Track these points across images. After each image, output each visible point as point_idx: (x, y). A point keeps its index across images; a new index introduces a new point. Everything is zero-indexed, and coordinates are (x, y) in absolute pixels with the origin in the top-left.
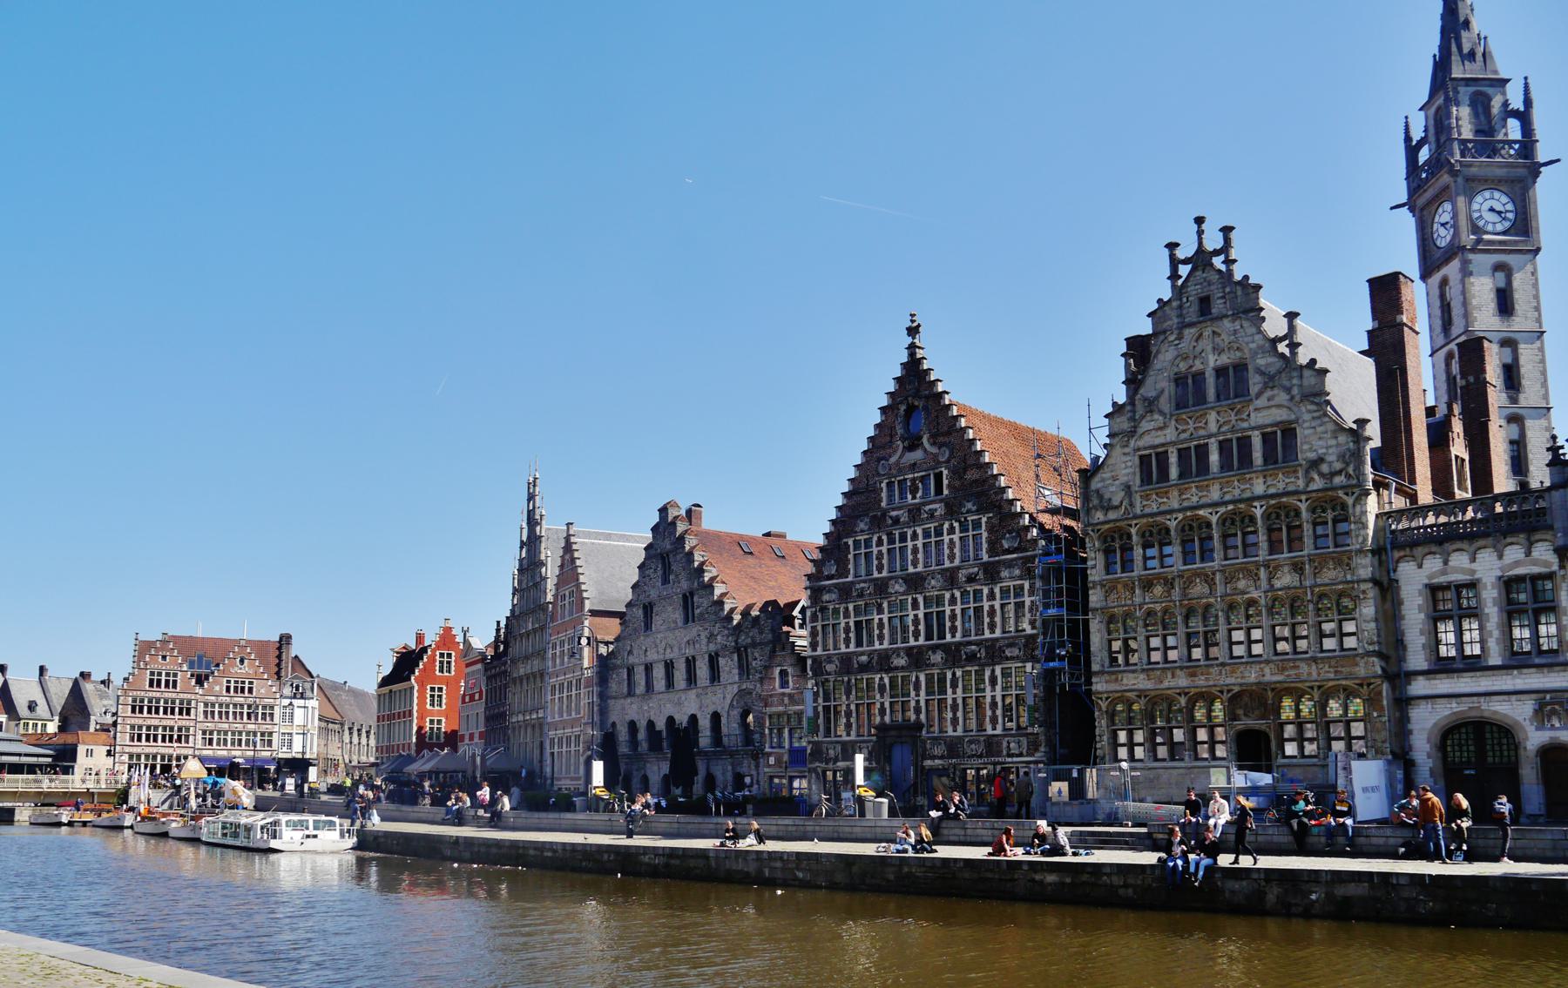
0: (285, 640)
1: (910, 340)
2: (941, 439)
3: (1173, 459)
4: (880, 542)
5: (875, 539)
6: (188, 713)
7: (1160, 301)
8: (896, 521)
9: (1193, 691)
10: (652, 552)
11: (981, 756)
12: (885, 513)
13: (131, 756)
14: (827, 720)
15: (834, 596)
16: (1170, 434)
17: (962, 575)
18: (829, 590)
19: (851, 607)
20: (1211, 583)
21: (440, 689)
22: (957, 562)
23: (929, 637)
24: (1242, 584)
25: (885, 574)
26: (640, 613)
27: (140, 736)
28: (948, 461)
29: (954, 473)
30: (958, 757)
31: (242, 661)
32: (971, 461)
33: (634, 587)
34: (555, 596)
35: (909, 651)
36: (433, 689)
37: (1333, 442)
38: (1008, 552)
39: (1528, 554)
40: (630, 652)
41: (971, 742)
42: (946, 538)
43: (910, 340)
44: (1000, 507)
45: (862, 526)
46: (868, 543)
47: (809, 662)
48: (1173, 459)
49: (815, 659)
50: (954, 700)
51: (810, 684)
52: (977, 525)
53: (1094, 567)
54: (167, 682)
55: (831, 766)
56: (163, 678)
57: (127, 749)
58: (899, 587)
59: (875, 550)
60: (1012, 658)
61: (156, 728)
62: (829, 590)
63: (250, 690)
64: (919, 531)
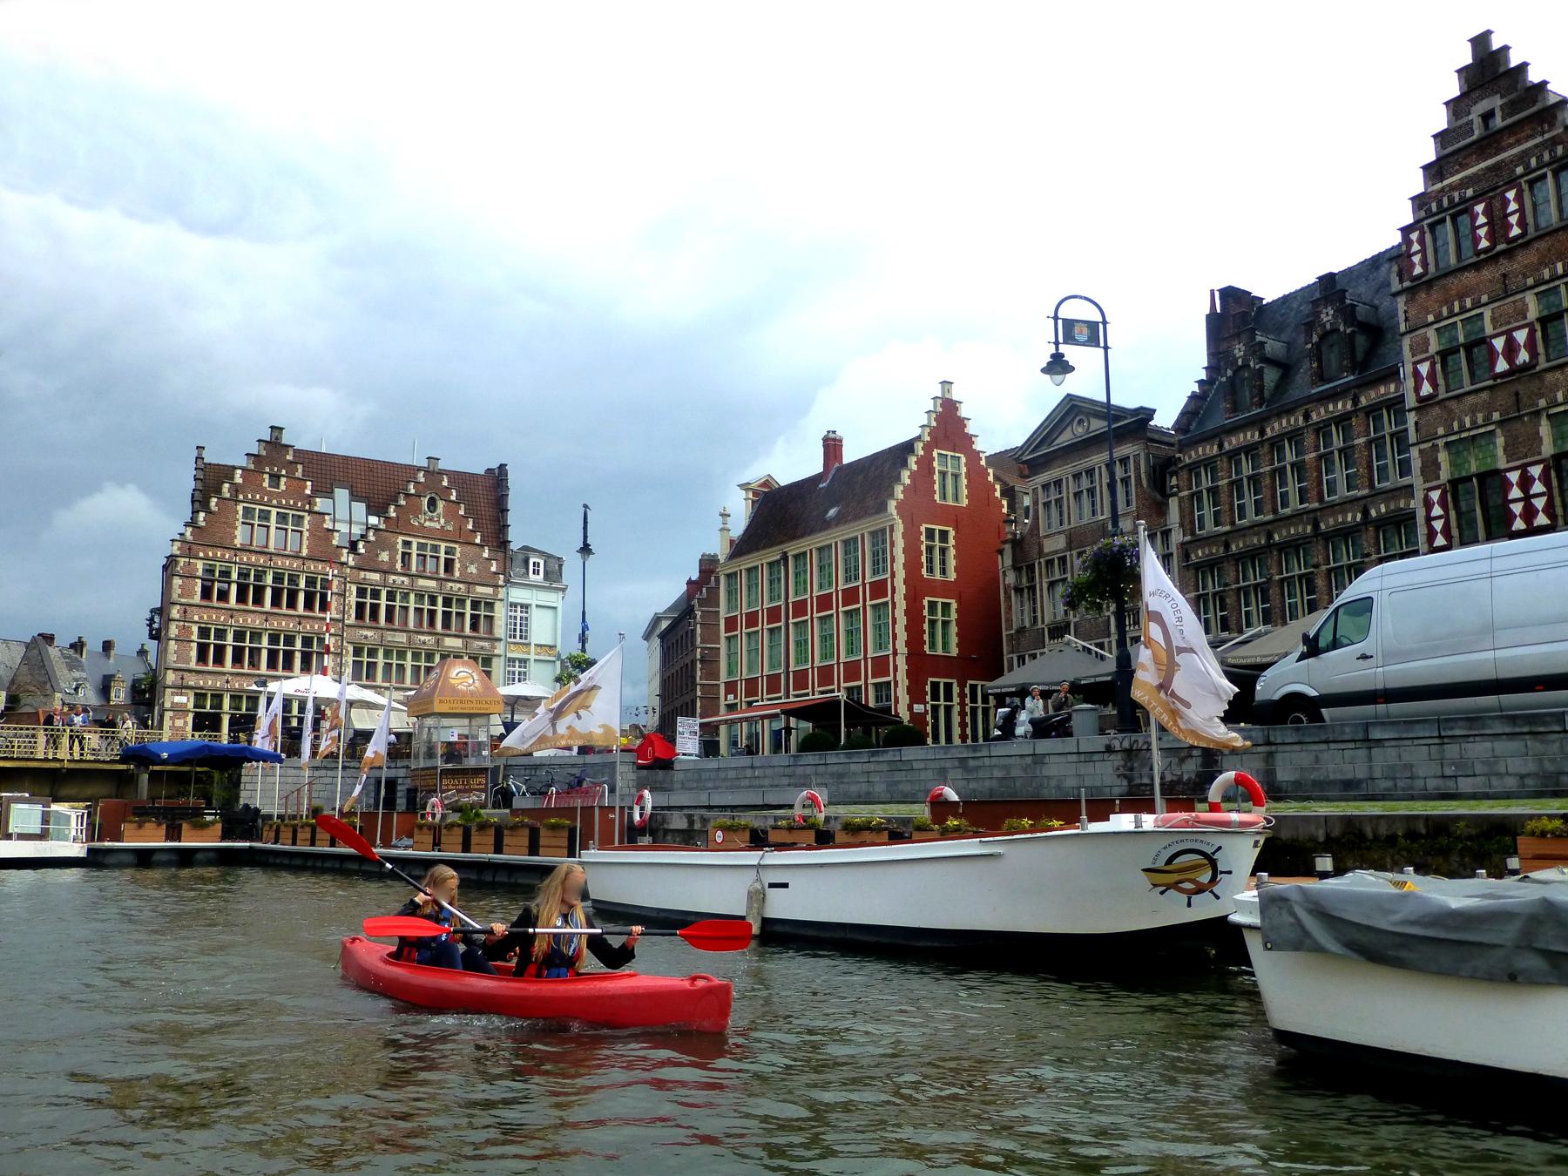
6: (325, 606)
13: (200, 697)
31: (432, 504)
36: (930, 534)
57: (192, 680)
63: (449, 565)
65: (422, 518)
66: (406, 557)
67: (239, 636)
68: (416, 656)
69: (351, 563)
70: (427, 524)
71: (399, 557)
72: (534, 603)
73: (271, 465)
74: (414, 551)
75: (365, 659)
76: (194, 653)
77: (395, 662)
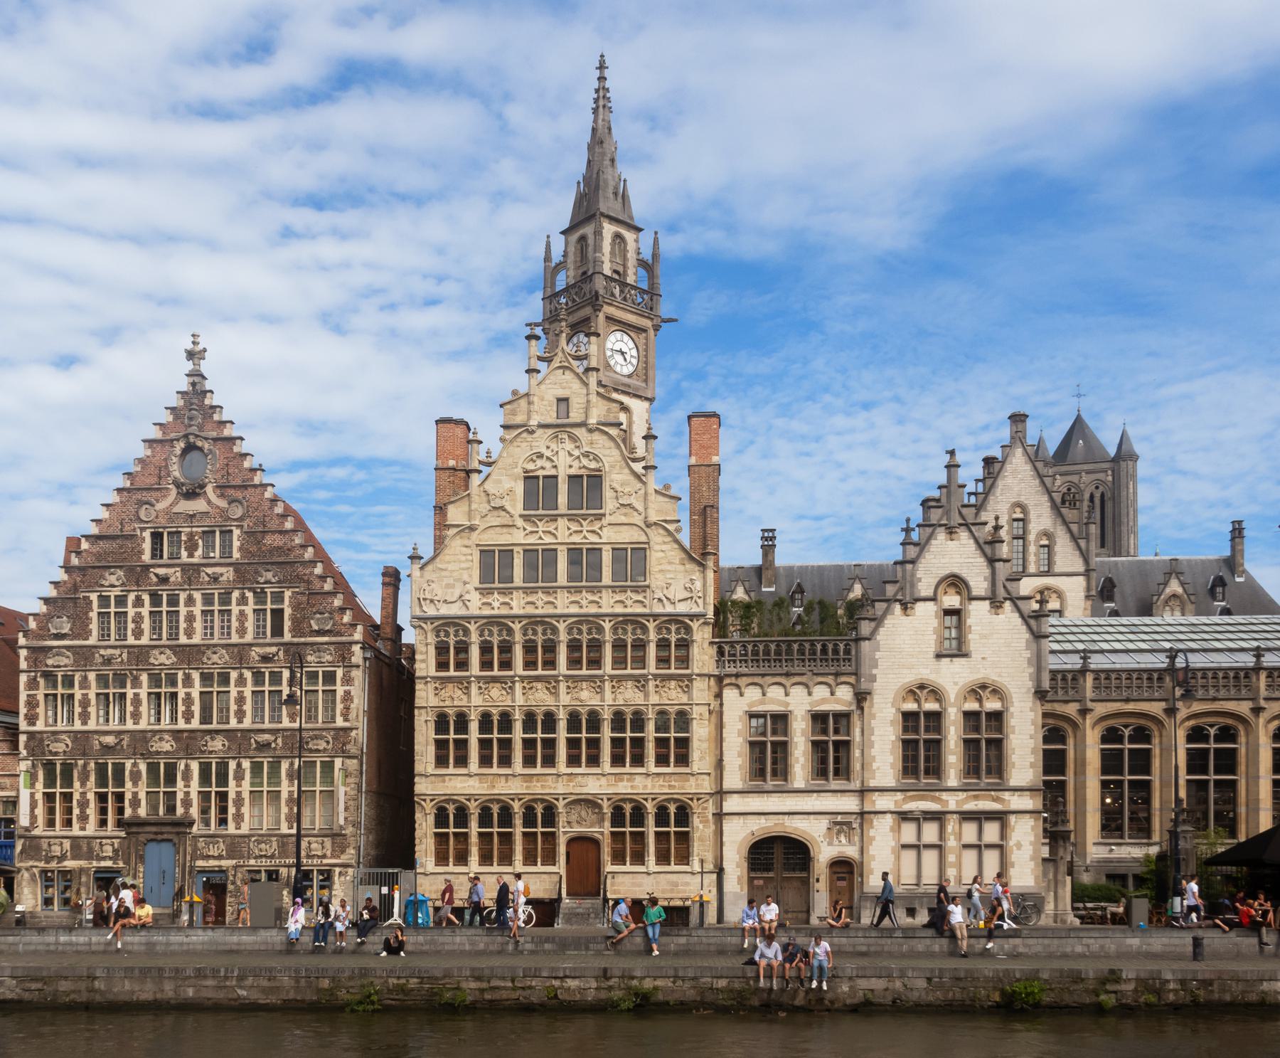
1: (189, 366)
2: (231, 492)
3: (518, 562)
4: (139, 602)
5: (131, 597)
7: (515, 393)
8: (164, 580)
9: (528, 798)
11: (272, 856)
12: (147, 568)
14: (51, 811)
15: (66, 661)
16: (518, 537)
17: (255, 653)
18: (58, 651)
19: (92, 676)
20: (555, 693)
22: (249, 638)
23: (206, 718)
24: (585, 695)
25: (145, 640)
28: (241, 519)
29: (249, 534)
30: (242, 857)
32: (273, 525)
35: (176, 734)
37: (682, 568)
38: (320, 633)
39: (832, 694)
41: (259, 842)
42: (235, 609)
43: (189, 366)
44: (309, 582)
45: (113, 579)
46: (121, 601)
47: (23, 739)
48: (518, 562)
49: (31, 735)
50: (239, 794)
51: (24, 766)
52: (278, 598)
53: (423, 661)
55: (53, 865)
58: (164, 659)
59: (131, 611)
60: (318, 751)
62: (58, 651)
64: (197, 596)
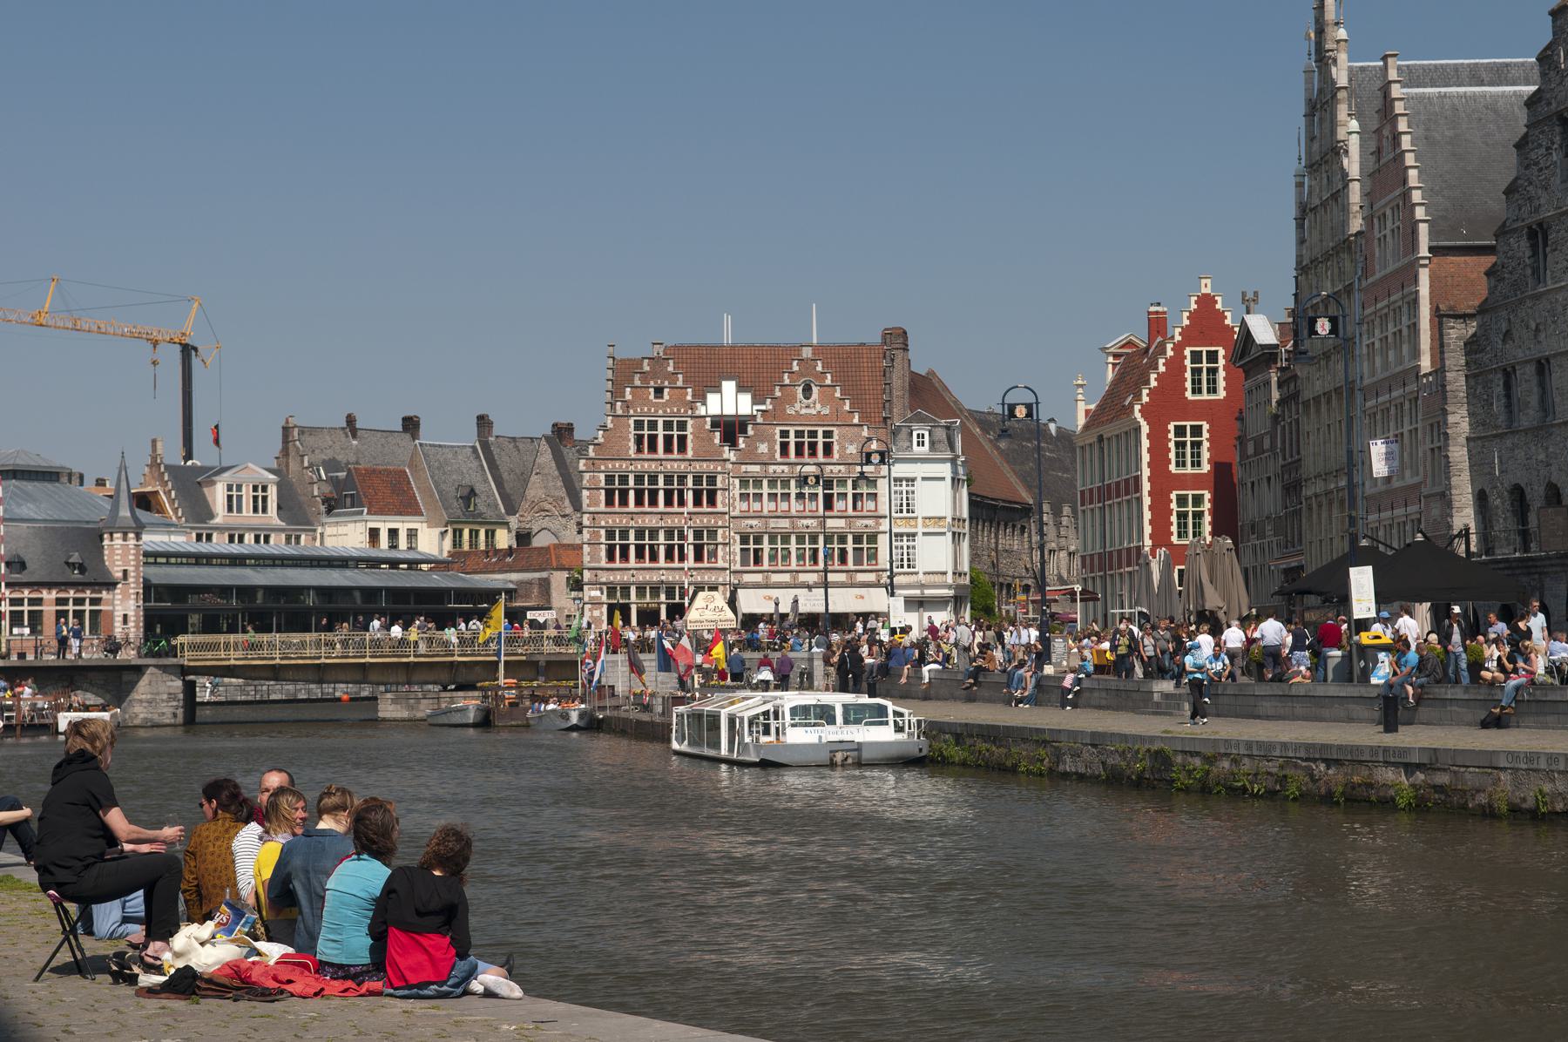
0: (897, 339)
6: (712, 502)
10: (1543, 110)
13: (611, 591)
21: (1197, 431)
26: (1522, 246)
27: (625, 550)
31: (807, 391)
33: (1509, 191)
34: (1369, 220)
36: (1180, 431)
40: (1507, 335)
54: (668, 439)
56: (660, 432)
57: (604, 577)
61: (654, 533)
63: (828, 449)
65: (798, 406)
66: (784, 447)
67: (640, 534)
68: (800, 540)
69: (733, 459)
70: (803, 411)
71: (778, 447)
72: (919, 476)
73: (654, 378)
74: (792, 439)
75: (752, 546)
76: (603, 554)
77: (779, 546)
